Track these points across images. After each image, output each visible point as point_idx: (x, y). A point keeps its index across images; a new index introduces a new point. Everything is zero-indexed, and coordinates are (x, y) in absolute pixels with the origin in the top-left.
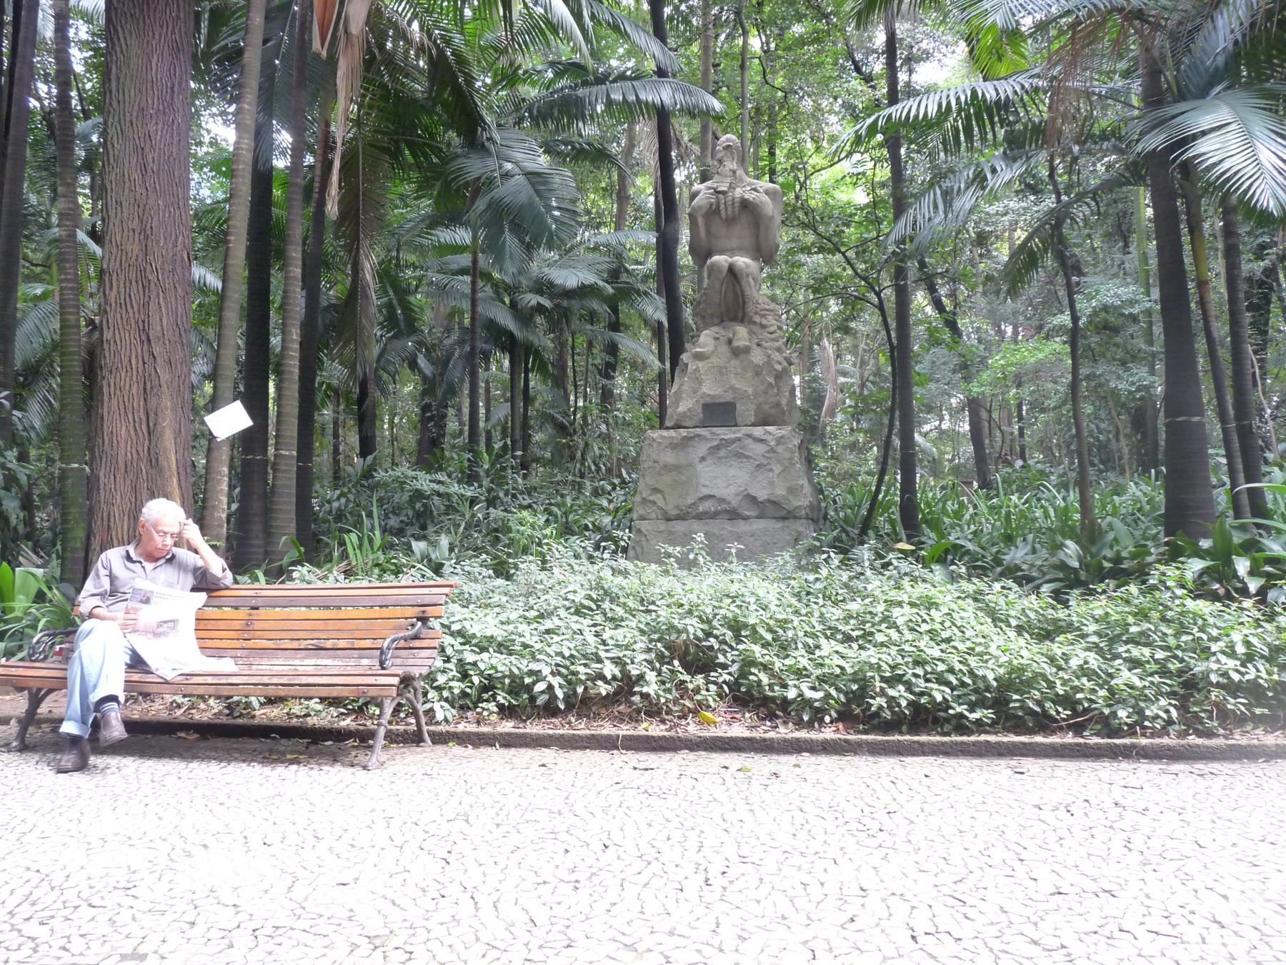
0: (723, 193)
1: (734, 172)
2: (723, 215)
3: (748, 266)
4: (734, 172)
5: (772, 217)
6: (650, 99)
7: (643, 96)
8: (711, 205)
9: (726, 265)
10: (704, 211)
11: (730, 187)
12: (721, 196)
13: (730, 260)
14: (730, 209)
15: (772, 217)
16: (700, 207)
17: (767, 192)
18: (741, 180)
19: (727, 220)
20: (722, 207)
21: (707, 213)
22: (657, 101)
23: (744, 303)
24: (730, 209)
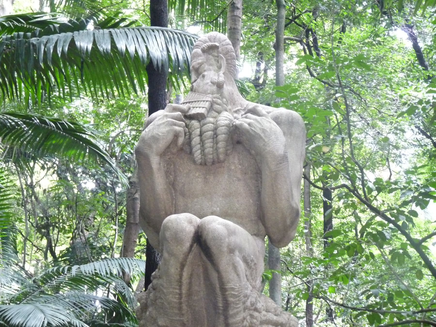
0: (199, 117)
1: (220, 86)
2: (197, 154)
3: (231, 233)
4: (220, 86)
5: (284, 158)
6: (132, 50)
7: (121, 45)
8: (176, 136)
9: (190, 230)
10: (162, 145)
11: (211, 108)
12: (195, 123)
13: (197, 220)
14: (209, 144)
15: (284, 158)
16: (155, 139)
17: (277, 120)
18: (233, 102)
19: (204, 164)
20: (196, 140)
21: (168, 147)
22: (142, 53)
23: (227, 305)
24: (209, 144)
